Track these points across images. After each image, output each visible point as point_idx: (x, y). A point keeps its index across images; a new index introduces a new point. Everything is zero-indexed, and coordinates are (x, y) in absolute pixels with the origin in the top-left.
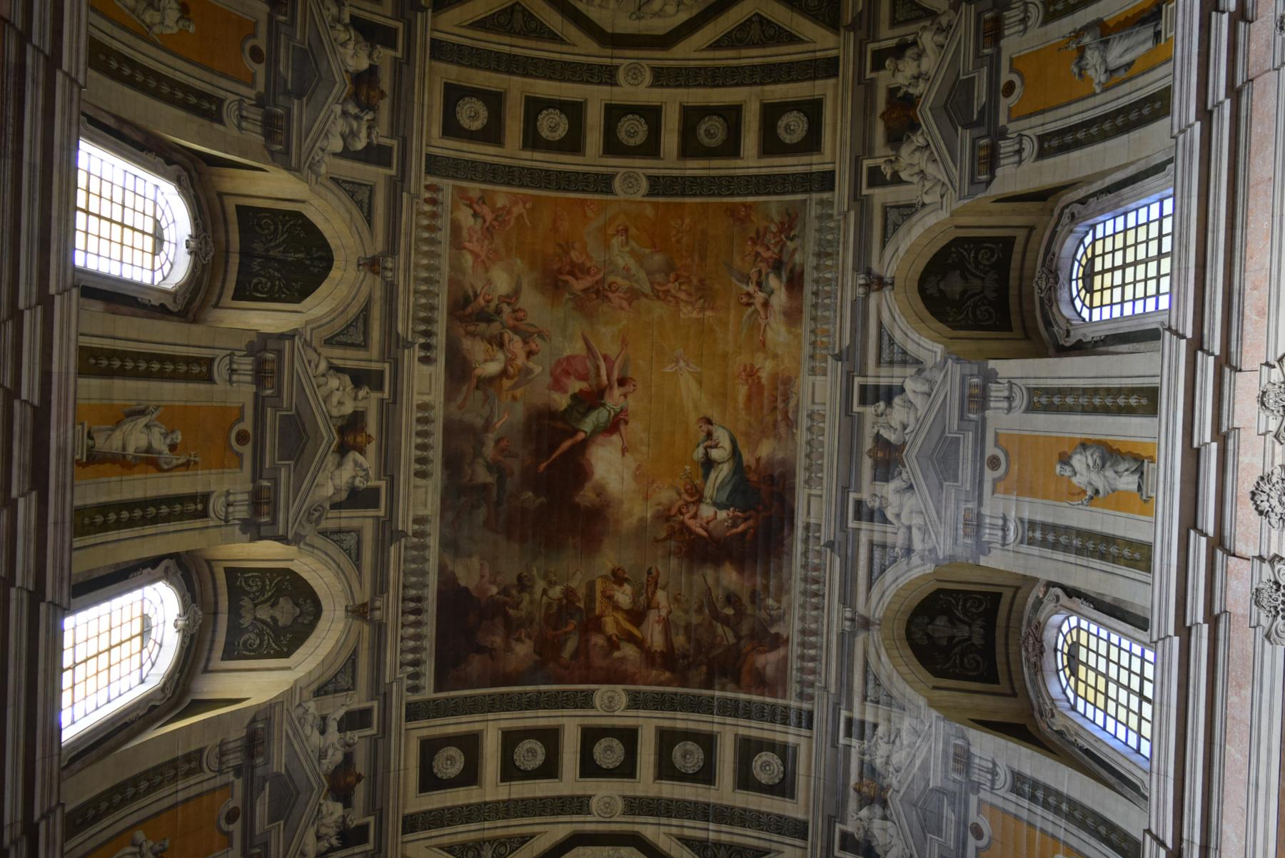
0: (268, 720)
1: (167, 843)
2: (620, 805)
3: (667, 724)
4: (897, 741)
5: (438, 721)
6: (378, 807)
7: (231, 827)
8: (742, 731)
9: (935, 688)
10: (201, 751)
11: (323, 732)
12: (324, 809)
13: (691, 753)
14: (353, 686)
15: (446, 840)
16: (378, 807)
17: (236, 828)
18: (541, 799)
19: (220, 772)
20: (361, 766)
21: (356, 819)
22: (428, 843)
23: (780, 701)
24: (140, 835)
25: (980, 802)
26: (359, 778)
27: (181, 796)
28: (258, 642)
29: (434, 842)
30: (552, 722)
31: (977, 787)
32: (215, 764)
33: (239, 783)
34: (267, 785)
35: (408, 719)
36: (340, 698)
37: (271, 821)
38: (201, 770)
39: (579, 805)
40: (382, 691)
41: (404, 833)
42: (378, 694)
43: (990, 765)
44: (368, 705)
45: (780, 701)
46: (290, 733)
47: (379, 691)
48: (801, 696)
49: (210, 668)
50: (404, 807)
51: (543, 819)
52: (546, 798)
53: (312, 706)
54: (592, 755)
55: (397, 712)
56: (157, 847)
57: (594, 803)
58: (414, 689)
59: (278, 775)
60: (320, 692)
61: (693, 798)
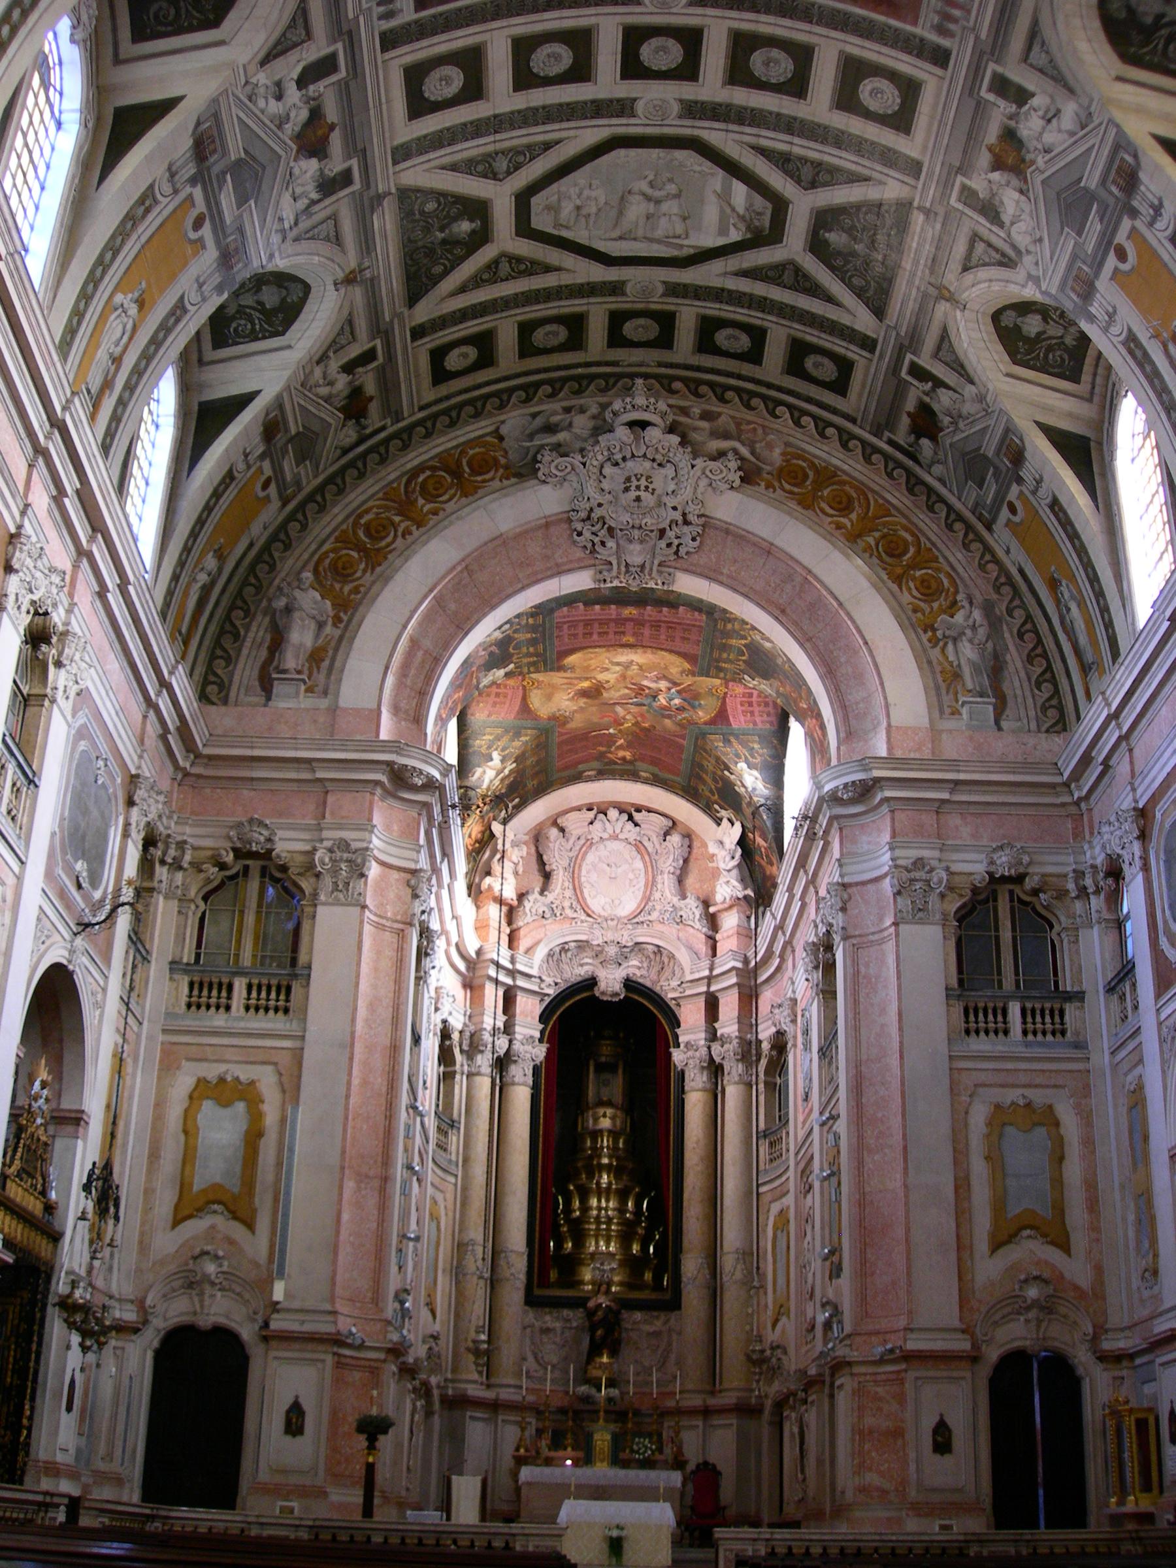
0: (216, 116)
1: (144, 285)
2: (676, 108)
3: (745, 26)
4: (1054, 121)
5: (425, 43)
6: (360, 146)
7: (200, 233)
8: (849, 49)
9: (1120, 79)
10: (151, 186)
11: (279, 97)
12: (296, 171)
13: (777, 62)
14: (309, 35)
15: (447, 160)
16: (360, 146)
17: (206, 231)
18: (568, 104)
19: (176, 192)
20: (332, 114)
21: (336, 164)
22: (426, 166)
23: (909, 28)
24: (119, 298)
25: (1133, 229)
26: (332, 127)
27: (143, 239)
28: (173, 11)
29: (433, 164)
30: (583, 22)
31: (1134, 213)
32: (167, 189)
33: (198, 193)
34: (228, 177)
35: (385, 48)
36: (293, 56)
37: (240, 205)
38: (156, 202)
39: (624, 108)
40: (345, 28)
41: (395, 163)
42: (340, 33)
43: (1156, 202)
44: (331, 49)
45: (909, 28)
46: (242, 115)
47: (345, 32)
48: (941, 30)
49: (122, 56)
50: (392, 139)
51: (572, 124)
52: (577, 103)
53: (262, 78)
54: (637, 55)
55: (368, 41)
56: (136, 294)
57: (640, 107)
58: (389, 15)
59: (239, 162)
60: (265, 61)
61: (776, 109)
